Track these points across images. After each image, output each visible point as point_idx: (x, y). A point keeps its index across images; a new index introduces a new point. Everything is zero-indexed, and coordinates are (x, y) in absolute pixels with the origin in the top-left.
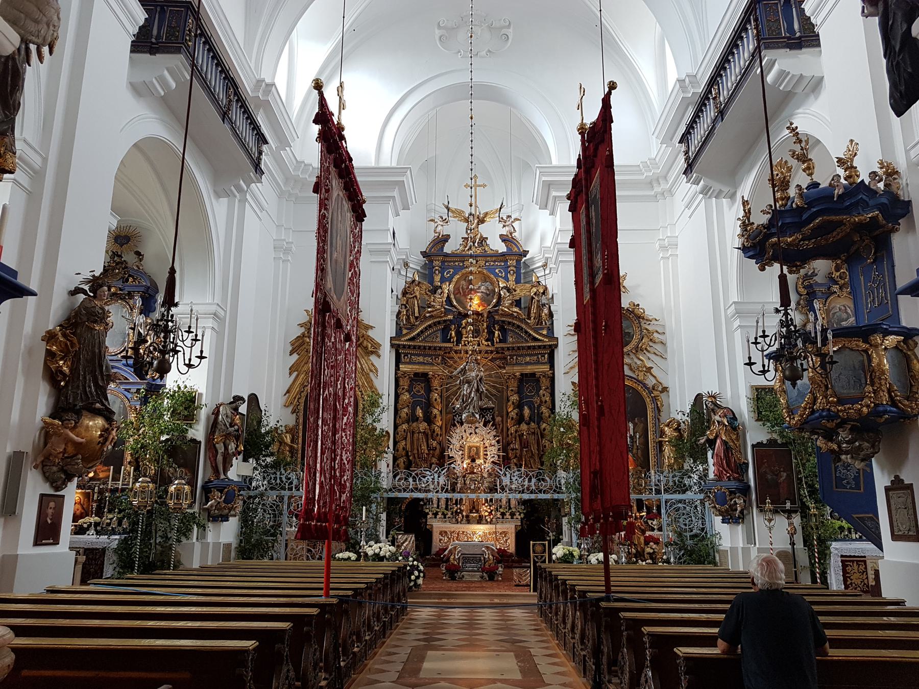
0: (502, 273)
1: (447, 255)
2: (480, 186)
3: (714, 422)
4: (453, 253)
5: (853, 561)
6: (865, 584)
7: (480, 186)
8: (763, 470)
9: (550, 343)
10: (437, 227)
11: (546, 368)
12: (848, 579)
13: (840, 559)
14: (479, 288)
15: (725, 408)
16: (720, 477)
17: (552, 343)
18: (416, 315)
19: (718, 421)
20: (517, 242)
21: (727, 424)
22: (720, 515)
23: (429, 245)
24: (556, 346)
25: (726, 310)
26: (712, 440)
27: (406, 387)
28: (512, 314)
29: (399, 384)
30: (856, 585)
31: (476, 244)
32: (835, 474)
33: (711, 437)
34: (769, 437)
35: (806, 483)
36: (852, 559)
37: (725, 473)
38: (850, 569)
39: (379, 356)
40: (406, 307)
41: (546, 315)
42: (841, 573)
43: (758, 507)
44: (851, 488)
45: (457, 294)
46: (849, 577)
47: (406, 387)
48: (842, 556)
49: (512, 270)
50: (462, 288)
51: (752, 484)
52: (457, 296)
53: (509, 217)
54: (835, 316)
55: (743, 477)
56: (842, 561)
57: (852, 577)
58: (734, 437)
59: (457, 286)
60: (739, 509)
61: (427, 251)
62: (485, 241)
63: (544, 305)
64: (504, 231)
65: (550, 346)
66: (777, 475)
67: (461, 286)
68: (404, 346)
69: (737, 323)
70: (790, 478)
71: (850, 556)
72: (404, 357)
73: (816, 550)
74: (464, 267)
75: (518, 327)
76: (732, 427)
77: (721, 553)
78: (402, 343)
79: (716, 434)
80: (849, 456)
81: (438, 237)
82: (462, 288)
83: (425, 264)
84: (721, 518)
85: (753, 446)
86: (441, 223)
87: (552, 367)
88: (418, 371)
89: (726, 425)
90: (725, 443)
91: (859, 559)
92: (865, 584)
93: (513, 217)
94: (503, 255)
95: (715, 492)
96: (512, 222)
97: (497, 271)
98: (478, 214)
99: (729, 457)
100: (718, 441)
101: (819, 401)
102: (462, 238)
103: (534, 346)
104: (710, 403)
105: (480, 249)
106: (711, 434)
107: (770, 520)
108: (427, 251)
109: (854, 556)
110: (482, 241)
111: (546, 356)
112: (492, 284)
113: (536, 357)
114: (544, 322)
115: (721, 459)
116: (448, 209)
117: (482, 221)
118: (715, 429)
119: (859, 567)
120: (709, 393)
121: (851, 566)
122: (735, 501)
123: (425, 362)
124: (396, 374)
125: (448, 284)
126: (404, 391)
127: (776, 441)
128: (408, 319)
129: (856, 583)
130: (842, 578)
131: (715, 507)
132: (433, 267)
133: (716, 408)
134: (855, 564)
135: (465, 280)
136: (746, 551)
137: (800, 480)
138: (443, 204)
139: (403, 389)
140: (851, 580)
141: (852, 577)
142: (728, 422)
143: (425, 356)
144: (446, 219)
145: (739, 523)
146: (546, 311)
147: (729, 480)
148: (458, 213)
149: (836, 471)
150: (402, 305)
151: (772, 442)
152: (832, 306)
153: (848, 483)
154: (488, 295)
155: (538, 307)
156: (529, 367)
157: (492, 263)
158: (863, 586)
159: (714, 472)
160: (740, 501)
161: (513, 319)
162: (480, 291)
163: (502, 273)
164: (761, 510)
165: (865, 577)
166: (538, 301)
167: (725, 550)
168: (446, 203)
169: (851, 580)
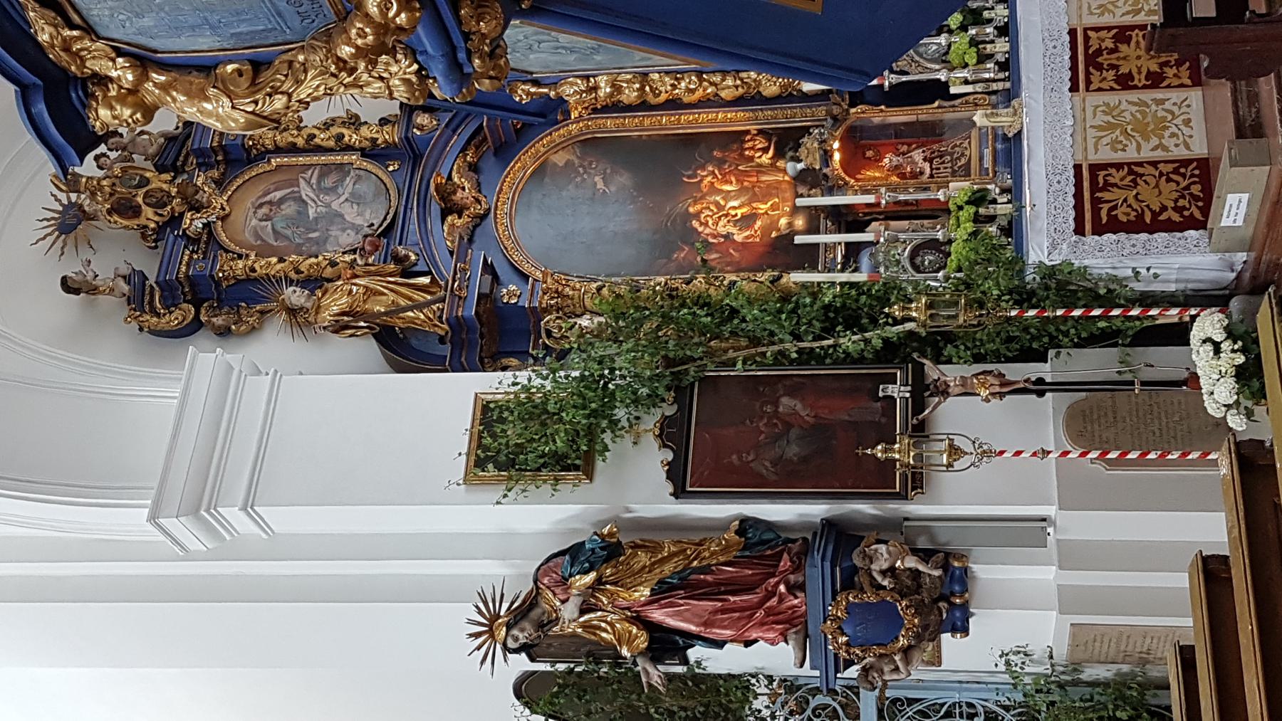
3: (585, 626)
5: (1096, 202)
6: (1176, 171)
8: (764, 467)
12: (1163, 217)
13: (1091, 239)
15: (535, 582)
16: (790, 622)
19: (583, 612)
21: (593, 575)
22: (935, 638)
25: (188, 555)
26: (652, 641)
30: (1183, 197)
33: (642, 641)
34: (650, 443)
35: (817, 338)
36: (1087, 206)
37: (774, 601)
38: (1124, 209)
42: (1144, 236)
43: (902, 496)
46: (1155, 215)
48: (1080, 230)
51: (816, 510)
54: (288, 232)
55: (794, 541)
56: (1099, 230)
57: (1156, 208)
58: (643, 558)
60: (911, 562)
66: (788, 426)
69: (233, 514)
70: (796, 388)
71: (1079, 207)
73: (1060, 312)
76: (607, 560)
77: (1080, 656)
79: (628, 619)
84: (946, 637)
85: (680, 492)
89: (599, 581)
90: (663, 592)
91: (1086, 184)
92: (1176, 171)
95: (848, 644)
99: (718, 584)
100: (657, 615)
104: (515, 632)
106: (630, 643)
107: (955, 451)
109: (1078, 196)
115: (723, 611)
118: (611, 624)
119: (1115, 185)
120: (477, 635)
121: (1115, 207)
122: (883, 573)
127: (666, 422)
129: (1175, 195)
130: (1161, 237)
131: (906, 651)
133: (535, 614)
134: (1106, 195)
136: (1071, 557)
137: (807, 357)
140: (1164, 208)
141: (1156, 208)
142: (586, 572)
145: (965, 570)
147: (802, 587)
151: (671, 434)
152: (252, 240)
158: (1184, 176)
159: (773, 642)
160: (883, 556)
164: (916, 482)
165: (1150, 170)
167: (1074, 636)
169: (1164, 208)
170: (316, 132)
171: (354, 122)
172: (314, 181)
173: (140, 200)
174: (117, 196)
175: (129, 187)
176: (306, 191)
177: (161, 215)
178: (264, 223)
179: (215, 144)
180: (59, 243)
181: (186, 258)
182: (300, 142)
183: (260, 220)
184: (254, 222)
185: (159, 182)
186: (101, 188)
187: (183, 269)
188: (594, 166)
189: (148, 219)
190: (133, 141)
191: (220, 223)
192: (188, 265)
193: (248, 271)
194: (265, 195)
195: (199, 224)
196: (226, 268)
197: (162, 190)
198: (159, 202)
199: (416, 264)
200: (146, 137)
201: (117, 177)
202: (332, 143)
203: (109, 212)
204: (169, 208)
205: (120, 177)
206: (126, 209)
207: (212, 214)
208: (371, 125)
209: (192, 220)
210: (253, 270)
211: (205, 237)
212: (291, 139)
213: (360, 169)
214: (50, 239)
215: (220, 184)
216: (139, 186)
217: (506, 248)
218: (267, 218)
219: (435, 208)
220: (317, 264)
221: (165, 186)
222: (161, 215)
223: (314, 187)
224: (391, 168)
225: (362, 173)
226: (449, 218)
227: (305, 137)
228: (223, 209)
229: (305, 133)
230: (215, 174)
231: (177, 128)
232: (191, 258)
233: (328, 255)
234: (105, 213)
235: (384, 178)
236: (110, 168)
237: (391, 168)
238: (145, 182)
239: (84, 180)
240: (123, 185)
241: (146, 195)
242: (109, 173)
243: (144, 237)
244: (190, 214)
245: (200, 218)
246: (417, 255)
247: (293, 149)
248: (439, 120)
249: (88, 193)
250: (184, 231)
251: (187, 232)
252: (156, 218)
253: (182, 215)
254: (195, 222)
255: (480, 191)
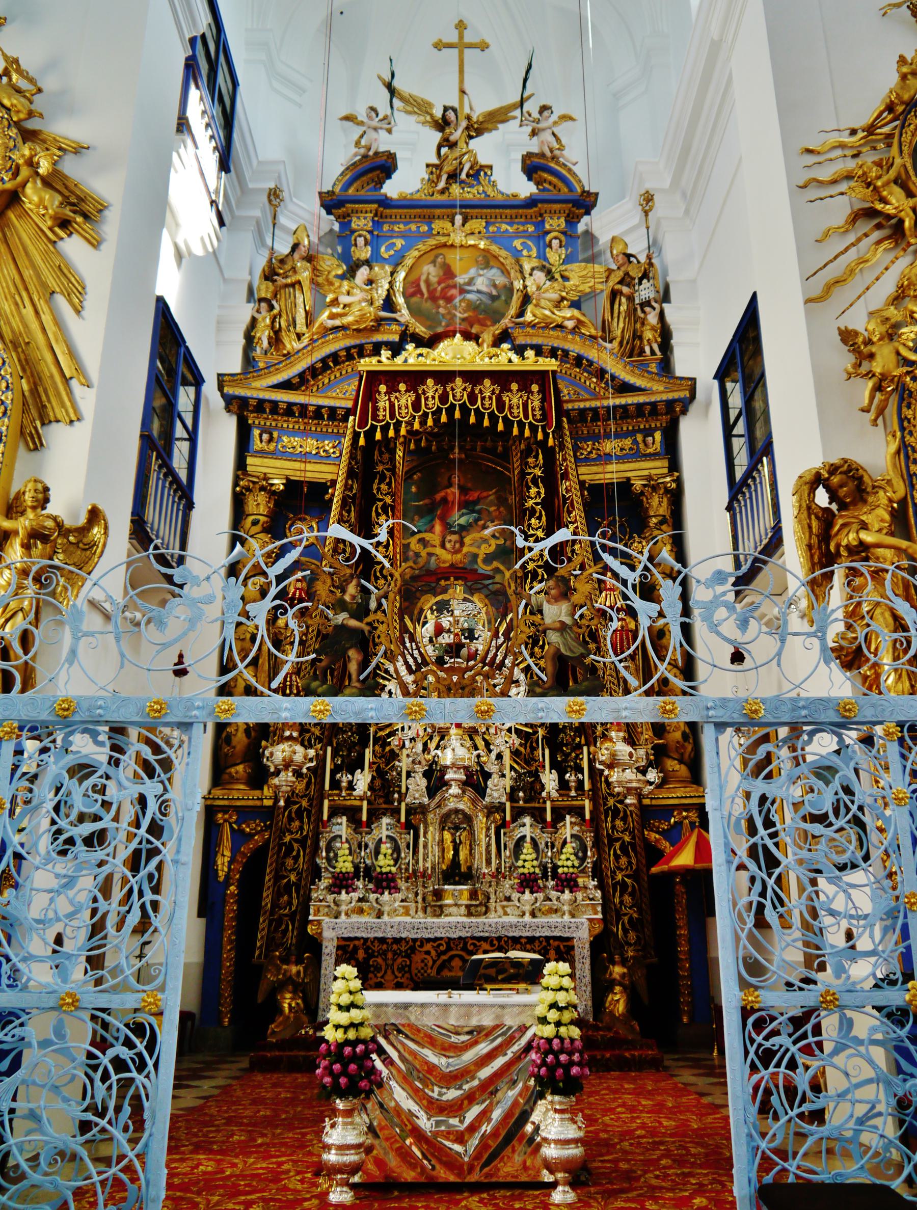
0: (529, 249)
1: (385, 202)
2: (471, 46)
4: (405, 198)
7: (471, 46)
9: (671, 396)
10: (362, 136)
11: (658, 467)
14: (471, 282)
17: (676, 395)
18: (298, 330)
20: (570, 170)
23: (342, 174)
24: (685, 404)
27: (262, 519)
28: (560, 327)
29: (243, 512)
31: (463, 176)
39: (96, 244)
40: (271, 307)
41: (653, 329)
45: (413, 295)
47: (262, 519)
49: (556, 238)
50: (427, 282)
52: (415, 299)
53: (544, 109)
59: (412, 277)
61: (337, 190)
62: (485, 174)
63: (647, 303)
64: (534, 146)
65: (670, 404)
67: (424, 278)
68: (260, 406)
72: (261, 435)
74: (430, 234)
75: (579, 360)
78: (255, 394)
81: (365, 156)
82: (427, 282)
83: (331, 230)
86: (375, 122)
87: (674, 466)
88: (296, 476)
93: (557, 112)
94: (531, 202)
96: (555, 123)
97: (517, 244)
98: (467, 110)
102: (428, 166)
103: (624, 407)
105: (474, 190)
108: (337, 190)
110: (478, 172)
111: (658, 435)
112: (505, 272)
113: (628, 442)
114: (647, 349)
116: (390, 87)
117: (476, 129)
123: (322, 454)
124: (236, 484)
125: (388, 269)
126: (258, 528)
128: (276, 340)
132: (353, 232)
135: (434, 262)
138: (379, 77)
139: (255, 523)
143: (321, 436)
144: (385, 118)
146: (652, 318)
148: (419, 106)
150: (261, 300)
154: (494, 298)
155: (631, 313)
156: (612, 467)
157: (504, 227)
161: (565, 339)
162: (474, 288)
163: (529, 249)
166: (630, 299)
168: (387, 77)
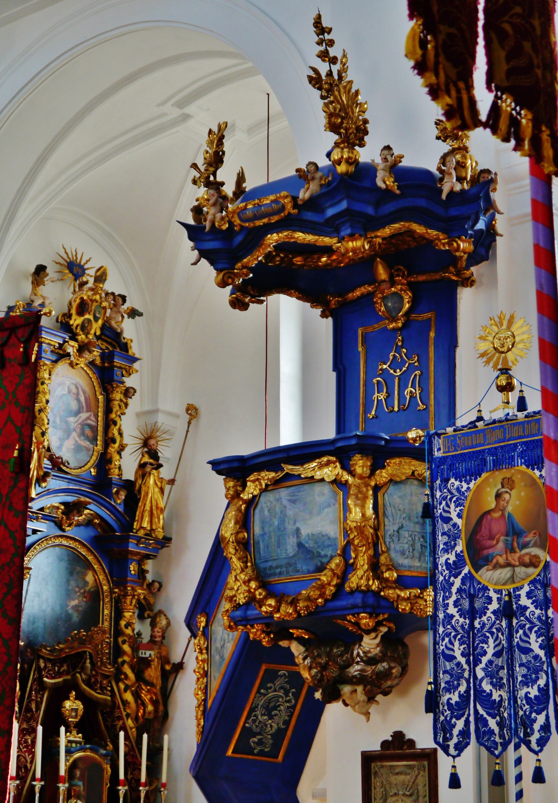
32: (245, 722)
44: (261, 753)
80: (360, 689)
101: (360, 573)
149: (248, 717)
153: (260, 743)
170: (117, 427)
171: (122, 448)
172: (89, 422)
173: (87, 316)
174: (90, 303)
175: (95, 311)
176: (84, 415)
177: (76, 328)
178: (66, 389)
179: (115, 364)
180: (62, 262)
181: (53, 343)
182: (113, 416)
183: (69, 388)
184: (68, 383)
185: (96, 327)
186: (95, 294)
187: (47, 341)
188: (84, 599)
189: (75, 320)
190: (119, 312)
191: (69, 362)
192: (49, 344)
193: (42, 380)
194: (84, 392)
195: (70, 350)
196: (45, 367)
197: (91, 330)
198: (85, 327)
199: (40, 486)
200: (120, 319)
201: (101, 303)
202: (110, 435)
203: (82, 299)
204: (81, 333)
205: (100, 306)
206: (82, 308)
207: (75, 358)
208: (119, 461)
209: (73, 347)
210: (43, 383)
211: (61, 352)
212: (115, 410)
213: (94, 451)
214: (65, 256)
215: (92, 364)
216: (95, 317)
217: (42, 542)
218: (70, 392)
219: (70, 499)
220: (43, 424)
221: (92, 332)
222: (76, 328)
223: (85, 422)
224: (92, 470)
225: (91, 453)
226: (62, 507)
227: (115, 419)
228: (77, 364)
229: (117, 419)
230: (98, 361)
231: (124, 338)
232: (52, 345)
233: (49, 431)
234: (82, 296)
235: (87, 467)
236: (106, 300)
237: (92, 470)
238: (96, 319)
239: (101, 286)
240: (97, 306)
241: (89, 321)
242: (103, 299)
243: (64, 315)
244: (77, 346)
245: (74, 352)
246: (45, 487)
247: (108, 410)
248: (120, 504)
249: (94, 287)
250: (67, 342)
251: (67, 344)
252: (75, 325)
253: (76, 340)
254: (71, 348)
255: (76, 526)
